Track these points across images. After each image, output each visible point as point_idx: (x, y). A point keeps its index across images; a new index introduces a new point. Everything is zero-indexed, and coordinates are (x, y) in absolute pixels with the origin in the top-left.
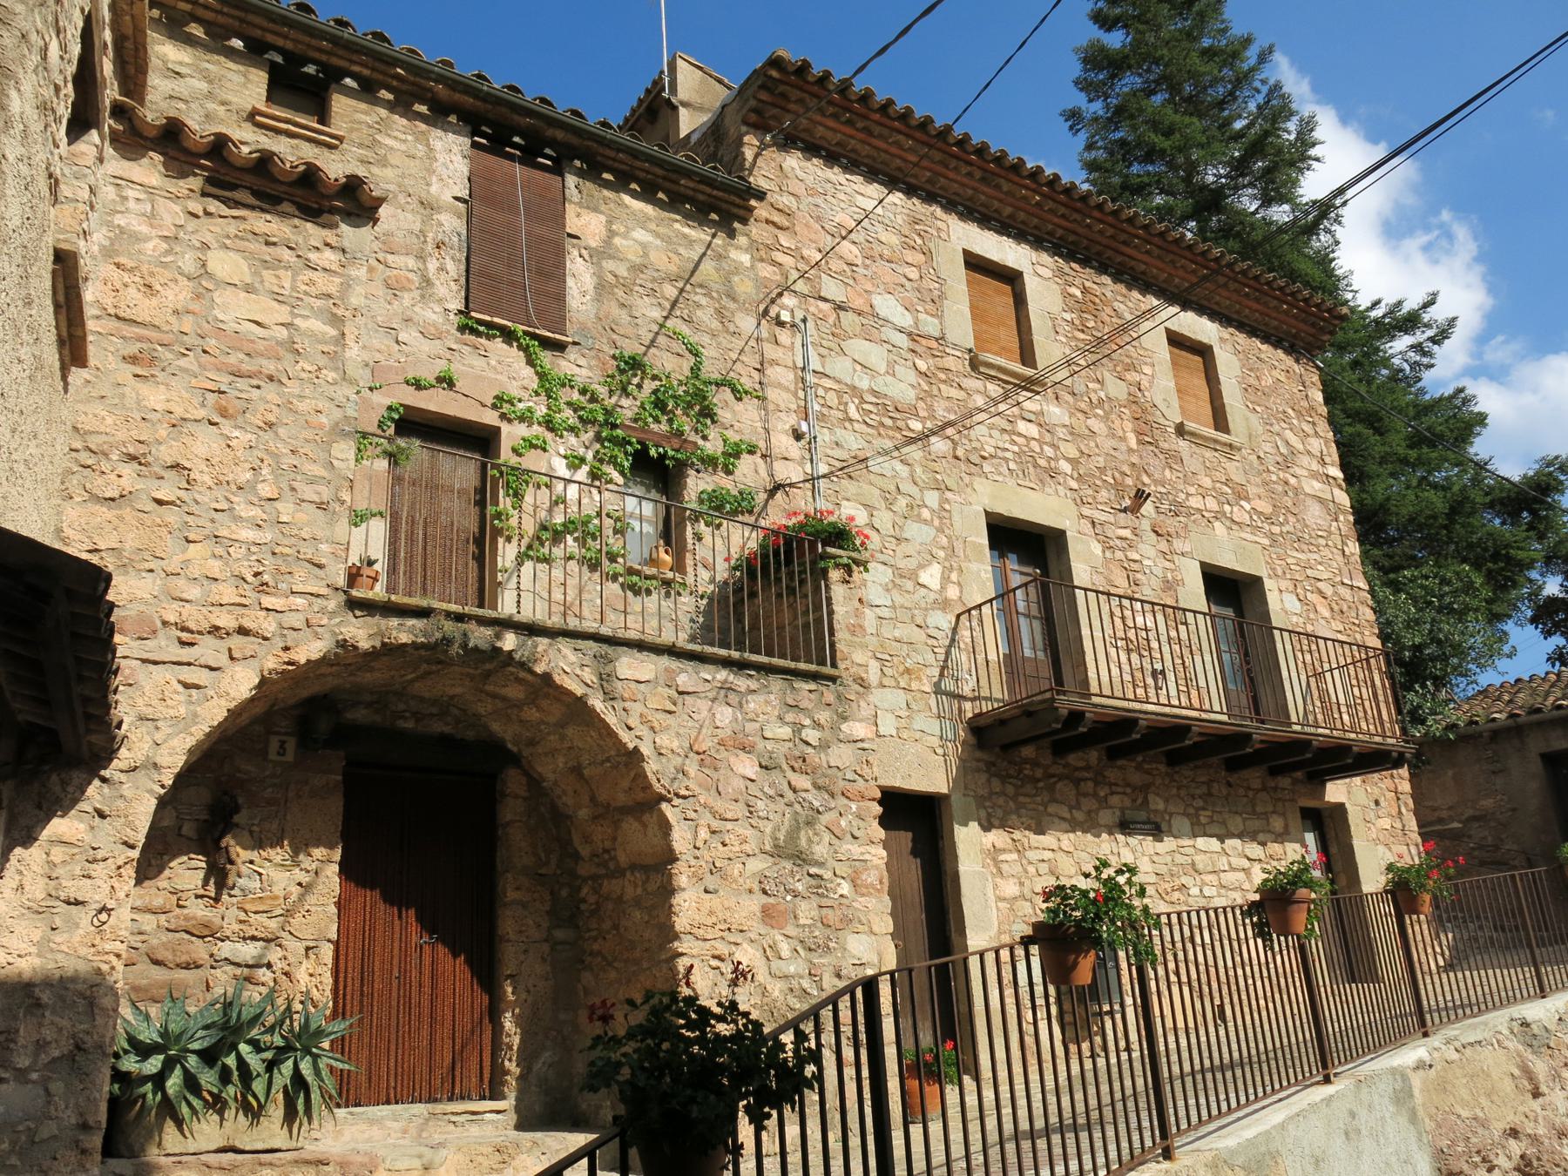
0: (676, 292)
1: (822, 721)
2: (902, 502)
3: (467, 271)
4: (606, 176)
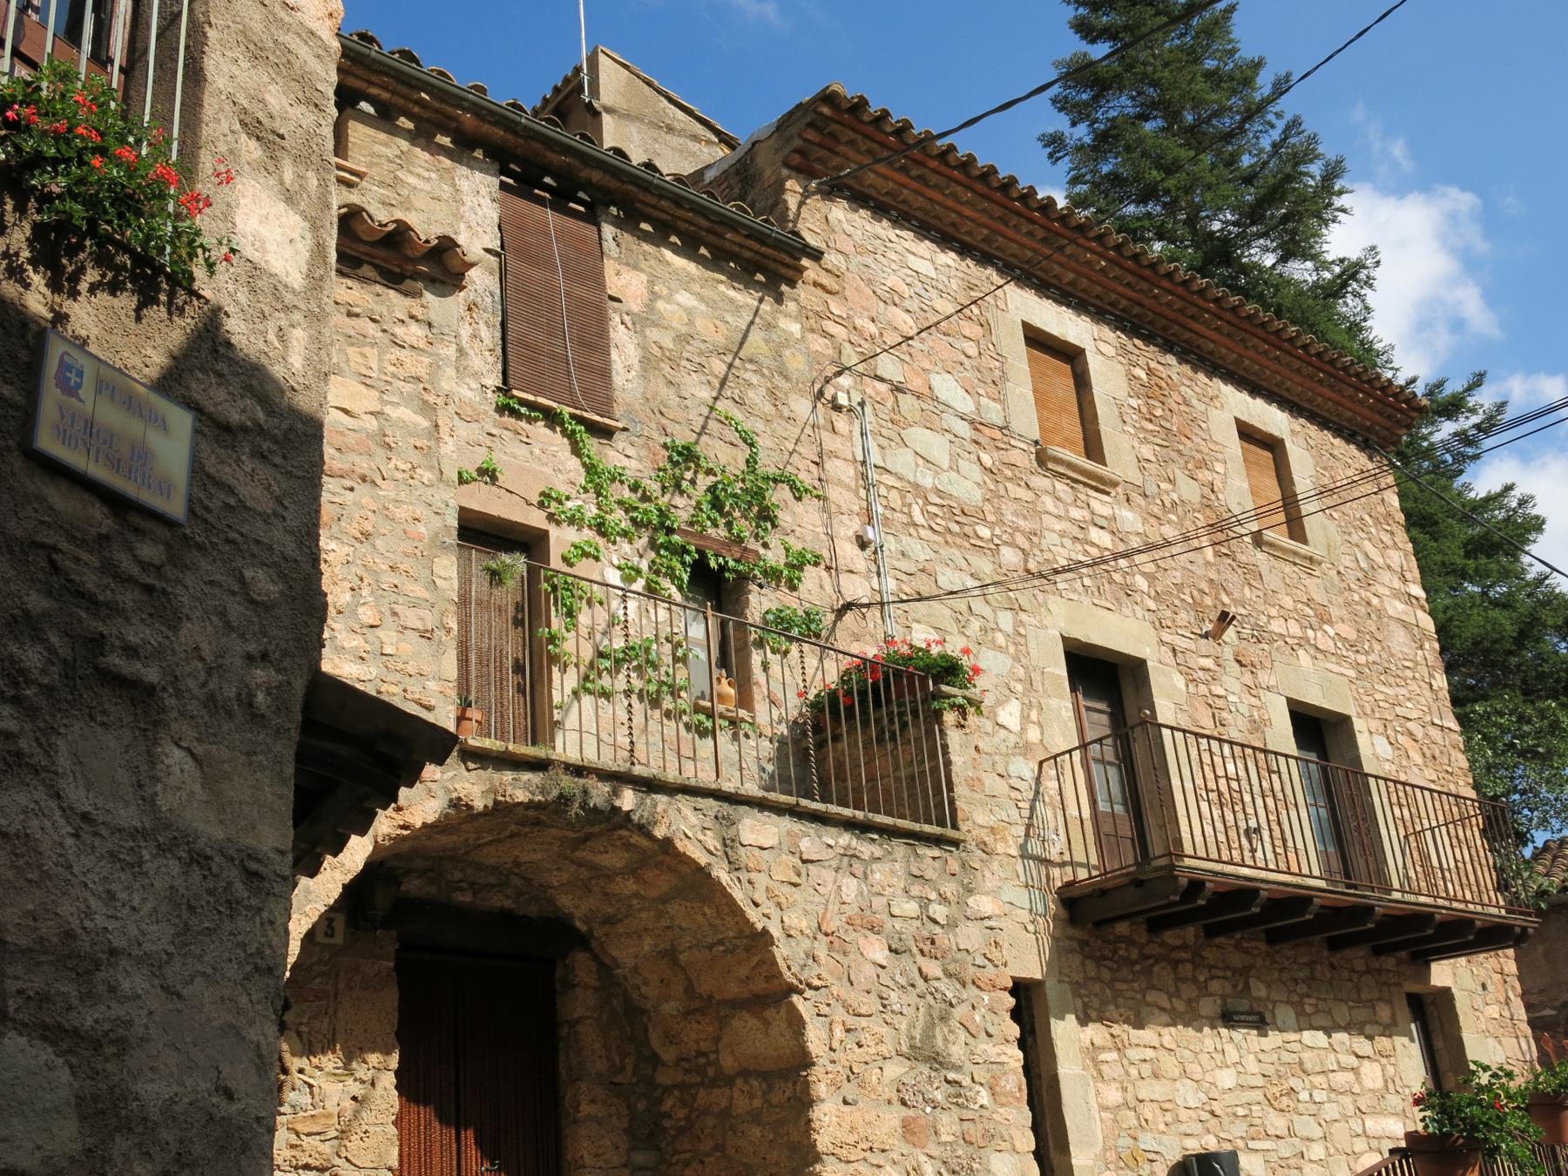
0: (724, 368)
1: (949, 895)
2: (975, 625)
3: (504, 338)
4: (645, 226)
